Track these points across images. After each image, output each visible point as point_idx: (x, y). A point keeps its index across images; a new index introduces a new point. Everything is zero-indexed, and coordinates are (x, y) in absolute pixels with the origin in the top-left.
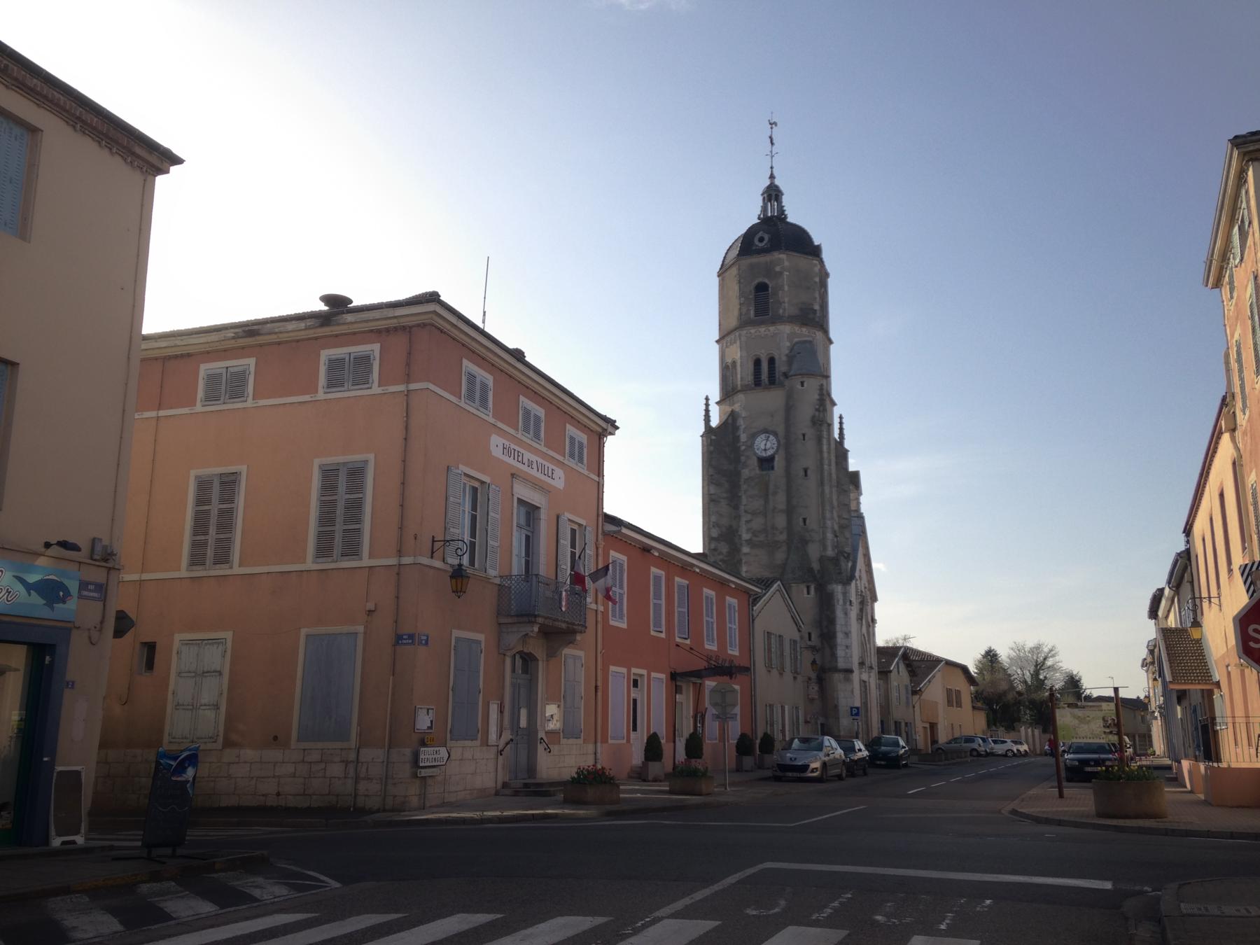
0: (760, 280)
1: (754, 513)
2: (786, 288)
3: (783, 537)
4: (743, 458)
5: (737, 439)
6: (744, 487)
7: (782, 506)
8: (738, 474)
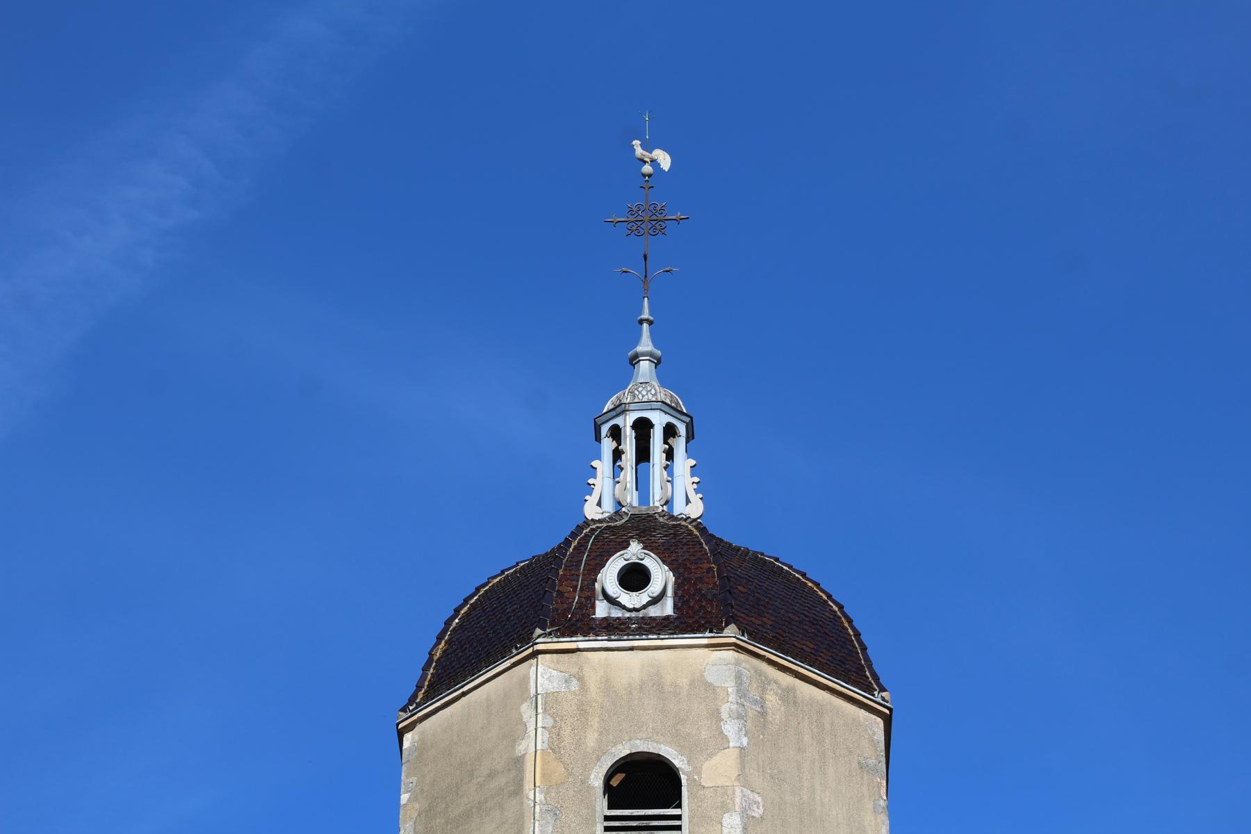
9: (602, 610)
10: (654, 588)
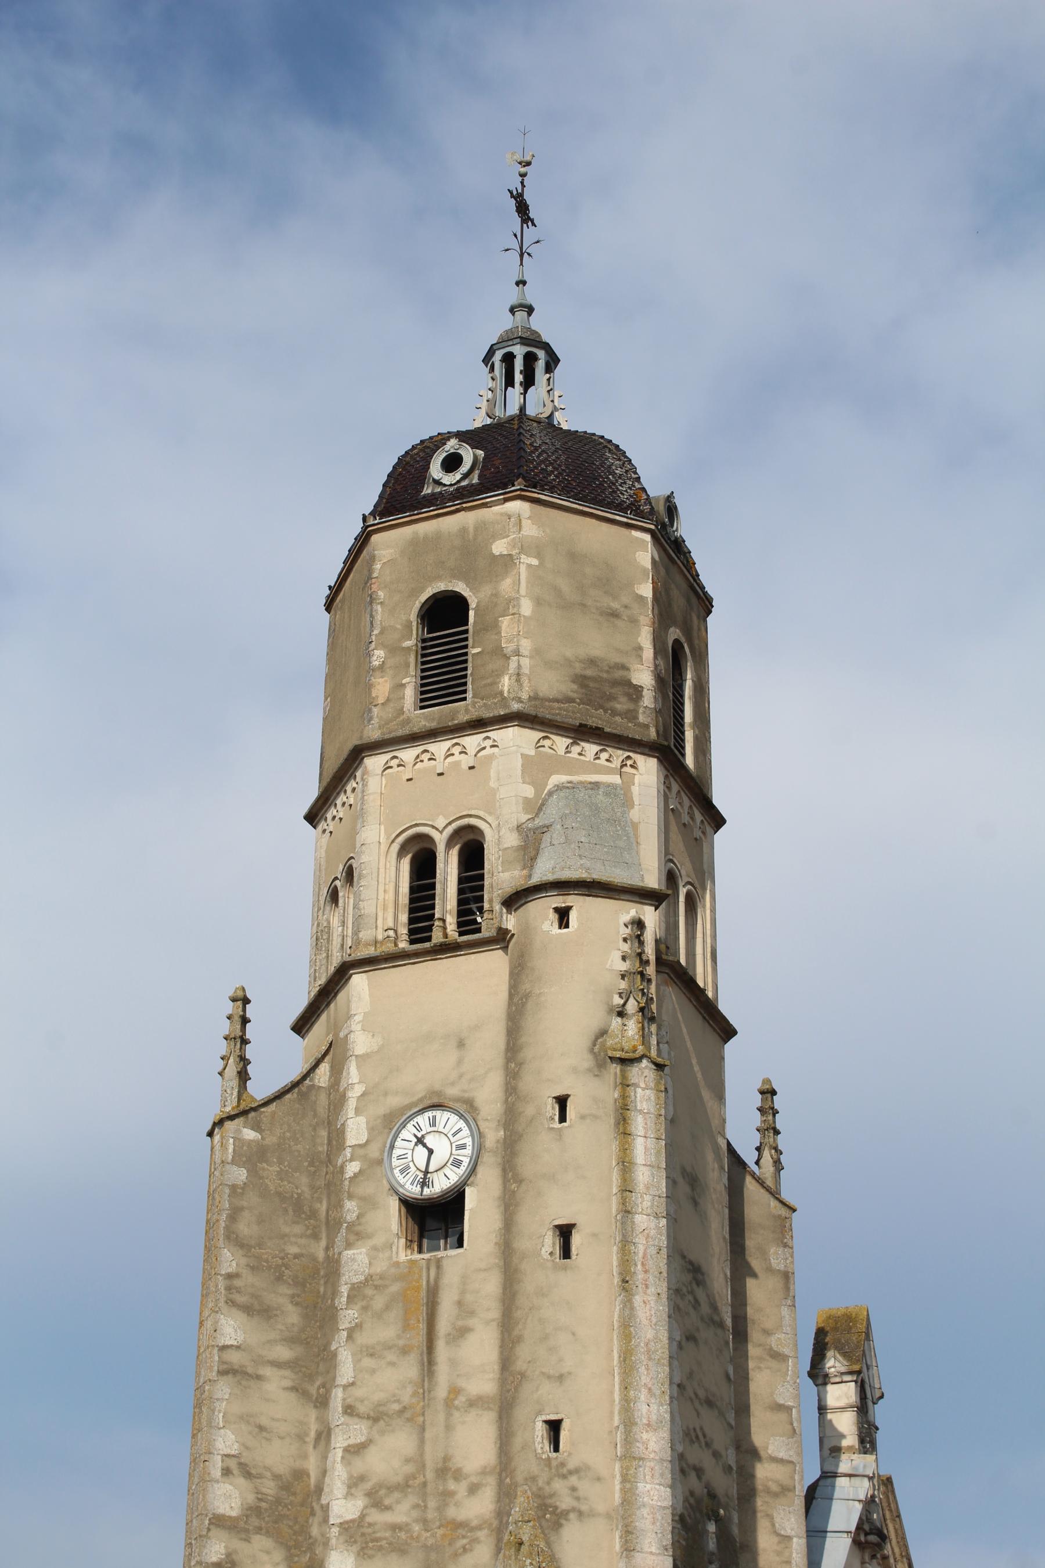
0: (441, 586)
1: (376, 1417)
2: (526, 608)
3: (479, 1507)
4: (351, 1208)
5: (337, 1137)
6: (348, 1316)
7: (484, 1384)
8: (332, 1268)
9: (427, 490)
10: (465, 468)
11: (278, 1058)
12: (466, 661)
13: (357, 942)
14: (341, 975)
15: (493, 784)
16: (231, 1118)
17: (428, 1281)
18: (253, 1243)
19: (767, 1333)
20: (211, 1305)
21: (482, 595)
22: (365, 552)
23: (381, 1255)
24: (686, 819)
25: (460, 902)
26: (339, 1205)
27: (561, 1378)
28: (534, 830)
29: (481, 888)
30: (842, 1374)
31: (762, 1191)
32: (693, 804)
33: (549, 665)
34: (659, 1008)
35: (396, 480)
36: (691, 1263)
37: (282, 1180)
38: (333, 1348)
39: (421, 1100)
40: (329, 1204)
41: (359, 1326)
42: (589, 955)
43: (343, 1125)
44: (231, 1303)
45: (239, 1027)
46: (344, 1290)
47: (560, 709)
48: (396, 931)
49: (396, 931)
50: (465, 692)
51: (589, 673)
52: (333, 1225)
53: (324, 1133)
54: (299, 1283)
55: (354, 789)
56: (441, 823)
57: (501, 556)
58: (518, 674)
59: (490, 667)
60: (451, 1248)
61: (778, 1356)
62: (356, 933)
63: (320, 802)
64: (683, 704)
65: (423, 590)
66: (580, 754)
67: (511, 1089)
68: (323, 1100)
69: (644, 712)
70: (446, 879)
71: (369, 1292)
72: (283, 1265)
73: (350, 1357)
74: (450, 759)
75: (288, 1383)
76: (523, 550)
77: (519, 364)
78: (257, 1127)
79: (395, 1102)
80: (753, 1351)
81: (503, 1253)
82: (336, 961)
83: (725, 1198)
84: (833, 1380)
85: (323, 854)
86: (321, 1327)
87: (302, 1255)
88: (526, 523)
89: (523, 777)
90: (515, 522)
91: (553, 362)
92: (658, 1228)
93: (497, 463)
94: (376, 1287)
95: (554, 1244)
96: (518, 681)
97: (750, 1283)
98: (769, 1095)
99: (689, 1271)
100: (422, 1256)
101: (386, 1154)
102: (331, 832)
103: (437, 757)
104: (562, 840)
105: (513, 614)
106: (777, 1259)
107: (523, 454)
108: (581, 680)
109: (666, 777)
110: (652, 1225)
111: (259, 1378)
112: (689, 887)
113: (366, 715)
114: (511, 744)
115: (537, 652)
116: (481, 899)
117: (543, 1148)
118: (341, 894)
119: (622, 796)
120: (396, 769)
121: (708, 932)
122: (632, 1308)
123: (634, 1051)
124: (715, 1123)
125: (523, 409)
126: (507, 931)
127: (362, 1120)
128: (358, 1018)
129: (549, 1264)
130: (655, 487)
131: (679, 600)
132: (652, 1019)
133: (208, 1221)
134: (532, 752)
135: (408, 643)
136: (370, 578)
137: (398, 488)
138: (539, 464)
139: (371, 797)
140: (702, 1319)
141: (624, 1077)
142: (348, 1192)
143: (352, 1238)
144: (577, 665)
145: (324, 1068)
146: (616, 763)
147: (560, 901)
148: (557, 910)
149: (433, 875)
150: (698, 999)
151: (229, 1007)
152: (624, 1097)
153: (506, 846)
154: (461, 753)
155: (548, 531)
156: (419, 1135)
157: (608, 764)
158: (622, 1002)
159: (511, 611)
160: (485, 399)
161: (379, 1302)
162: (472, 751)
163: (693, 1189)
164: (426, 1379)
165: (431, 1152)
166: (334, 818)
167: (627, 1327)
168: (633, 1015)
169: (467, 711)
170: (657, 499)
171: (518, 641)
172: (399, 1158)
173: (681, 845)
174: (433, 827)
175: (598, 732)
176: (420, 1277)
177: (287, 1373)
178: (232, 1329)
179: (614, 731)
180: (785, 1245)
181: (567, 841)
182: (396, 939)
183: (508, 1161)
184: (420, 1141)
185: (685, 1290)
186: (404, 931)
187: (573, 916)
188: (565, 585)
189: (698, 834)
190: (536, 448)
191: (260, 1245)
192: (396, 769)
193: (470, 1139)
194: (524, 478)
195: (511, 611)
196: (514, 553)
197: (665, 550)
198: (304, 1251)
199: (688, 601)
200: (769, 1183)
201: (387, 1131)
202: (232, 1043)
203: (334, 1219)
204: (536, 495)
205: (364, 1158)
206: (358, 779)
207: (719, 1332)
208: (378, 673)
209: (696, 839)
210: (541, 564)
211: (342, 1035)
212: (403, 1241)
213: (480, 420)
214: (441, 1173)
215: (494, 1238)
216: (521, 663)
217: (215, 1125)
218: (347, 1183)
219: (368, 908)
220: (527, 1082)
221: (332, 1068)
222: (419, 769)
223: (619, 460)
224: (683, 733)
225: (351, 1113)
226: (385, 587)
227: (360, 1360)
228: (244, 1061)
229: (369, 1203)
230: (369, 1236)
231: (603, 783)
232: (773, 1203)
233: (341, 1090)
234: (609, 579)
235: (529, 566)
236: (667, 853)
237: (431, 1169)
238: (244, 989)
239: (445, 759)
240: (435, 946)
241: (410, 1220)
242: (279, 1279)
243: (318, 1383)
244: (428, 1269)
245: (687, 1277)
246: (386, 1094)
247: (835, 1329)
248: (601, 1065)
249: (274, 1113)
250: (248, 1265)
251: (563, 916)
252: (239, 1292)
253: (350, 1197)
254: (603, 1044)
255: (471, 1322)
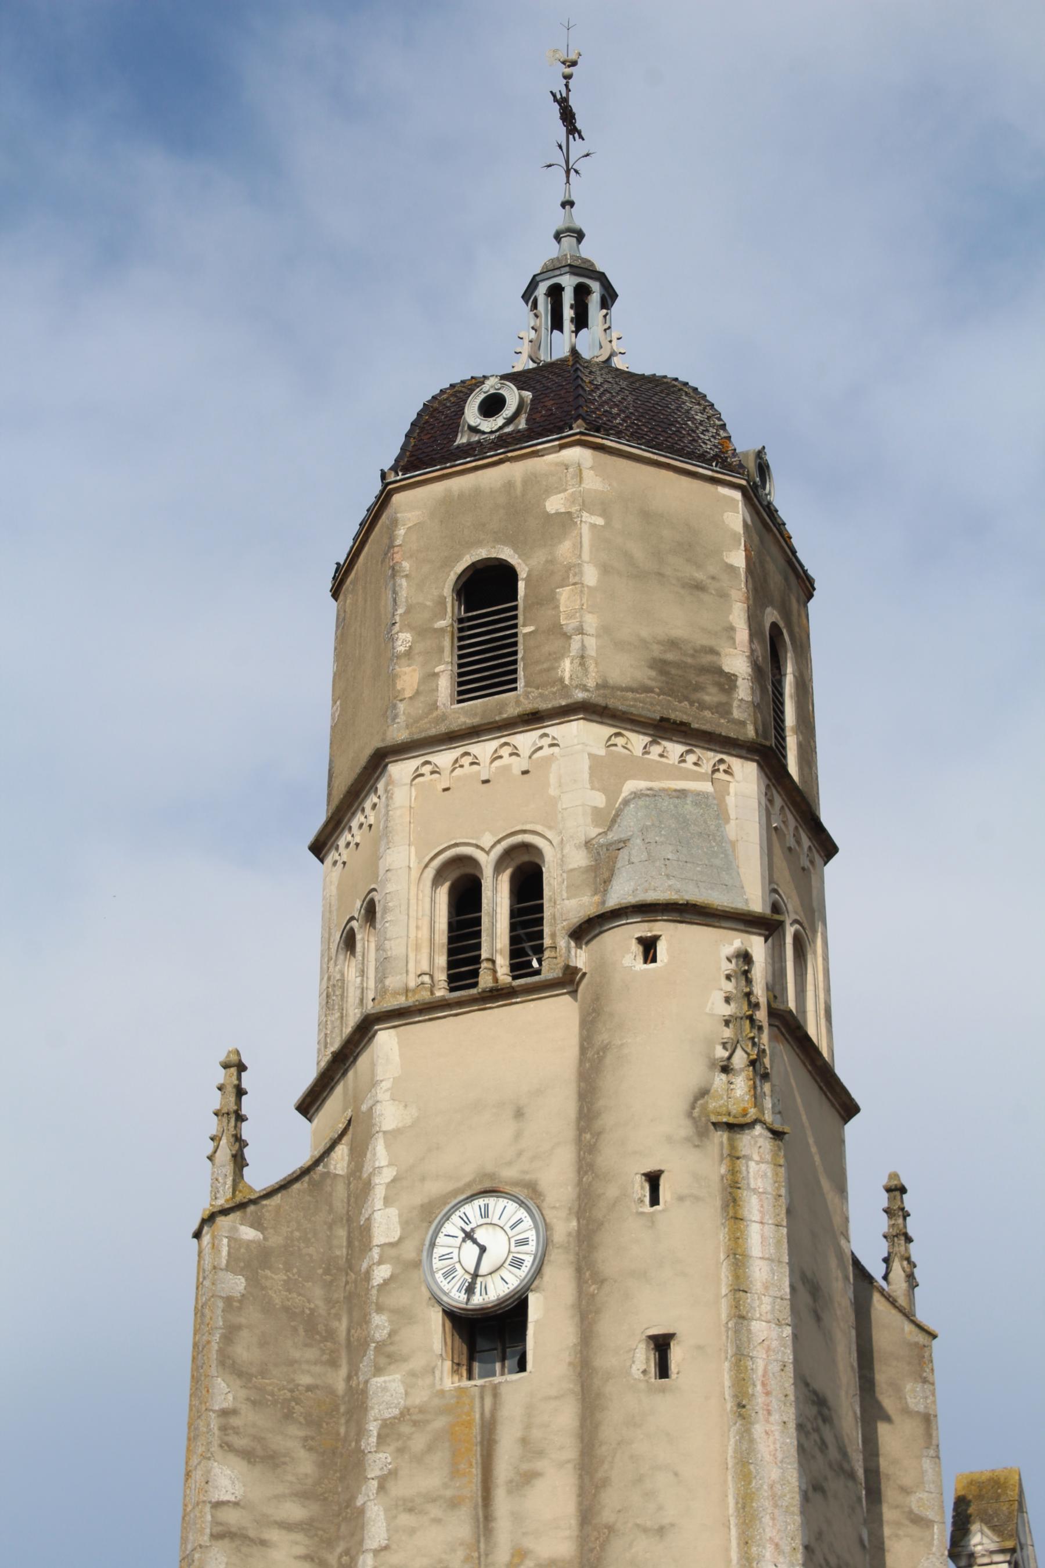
0: (482, 553)
2: (591, 576)
4: (380, 1324)
5: (360, 1236)
6: (379, 1462)
8: (357, 1401)
9: (462, 439)
11: (280, 1144)
12: (515, 644)
13: (382, 991)
14: (364, 1032)
15: (553, 791)
16: (225, 1212)
17: (482, 1414)
18: (254, 1370)
19: (905, 1491)
20: (200, 1450)
21: (533, 562)
22: (384, 517)
23: (420, 1382)
24: (791, 842)
25: (514, 940)
26: (365, 1320)
27: (661, 1531)
28: (608, 846)
29: (540, 921)
30: (992, 1552)
31: (894, 1311)
32: (801, 827)
33: (620, 646)
34: (772, 1061)
35: (422, 429)
36: (815, 1393)
37: (289, 1290)
38: (359, 1502)
39: (469, 1185)
40: (350, 1321)
41: (393, 1473)
42: (682, 995)
43: (368, 1219)
44: (227, 1447)
45: (233, 1099)
46: (373, 1428)
47: (635, 700)
48: (432, 977)
49: (432, 977)
50: (515, 681)
51: (670, 656)
52: (356, 1347)
53: (342, 1233)
54: (311, 1422)
55: (374, 806)
56: (487, 841)
57: (558, 514)
58: (582, 657)
59: (546, 649)
60: (510, 1372)
61: (918, 1520)
62: (380, 979)
63: (330, 826)
64: (782, 704)
65: (458, 559)
66: (661, 756)
67: (586, 1165)
68: (340, 1191)
69: (739, 706)
70: (494, 911)
71: (405, 1429)
72: (293, 1399)
73: (382, 1513)
74: (497, 763)
75: (301, 1550)
76: (584, 507)
77: (568, 298)
78: (257, 1224)
79: (435, 1188)
80: (888, 1514)
81: (580, 1375)
82: (353, 1017)
83: (852, 1317)
84: (980, 1561)
85: (334, 890)
86: (342, 1479)
87: (317, 1387)
88: (588, 474)
89: (591, 782)
90: (575, 474)
91: (609, 297)
92: (781, 1338)
93: (549, 404)
94: (415, 1423)
95: (648, 1360)
96: (582, 664)
97: (882, 1428)
98: (898, 1193)
99: (813, 1403)
100: (473, 1383)
101: (425, 1254)
102: (344, 863)
103: (481, 760)
104: (644, 856)
105: (574, 584)
106: (914, 1396)
107: (581, 392)
108: (660, 666)
109: (768, 787)
110: (774, 1335)
111: (263, 1543)
112: (797, 926)
113: (389, 712)
114: (576, 741)
115: (605, 631)
116: (540, 935)
117: (633, 1237)
118: (358, 937)
119: (714, 807)
120: (428, 777)
121: (821, 985)
122: (752, 1441)
123: (745, 1115)
124: (837, 1220)
125: (574, 351)
126: (575, 970)
127: (393, 1212)
128: (385, 1085)
129: (642, 1386)
130: (744, 442)
131: (776, 579)
132: (765, 1076)
133: (195, 1345)
134: (602, 752)
135: (442, 623)
136: (391, 546)
137: (425, 438)
138: (602, 405)
139: (398, 812)
140: (830, 1465)
141: (732, 1147)
142: (377, 1304)
143: (382, 1361)
144: (655, 647)
145: (342, 1151)
146: (707, 768)
147: (645, 930)
148: (640, 940)
149: (478, 907)
150: (813, 1062)
151: (220, 1076)
152: (733, 1172)
153: (571, 867)
154: (511, 755)
155: (615, 484)
156: (468, 1229)
157: (695, 768)
158: (726, 1054)
159: (572, 580)
160: (526, 341)
161: (419, 1442)
162: (525, 750)
163: (815, 1301)
164: (482, 1540)
165: (483, 1249)
166: (348, 844)
167: (745, 1465)
168: (742, 1070)
169: (518, 703)
170: (746, 454)
171: (581, 616)
172: (442, 1258)
173: (787, 874)
174: (478, 847)
175: (683, 728)
176: (472, 1408)
177: (299, 1537)
178: (228, 1480)
179: (704, 727)
180: (925, 1381)
181: (650, 858)
182: (433, 986)
183: (585, 1257)
184: (469, 1236)
185: (809, 1426)
186: (442, 976)
187: (661, 948)
188: (638, 552)
189: (806, 863)
190: (597, 387)
191: (263, 1373)
192: (428, 777)
193: (534, 1232)
194: (584, 419)
195: (572, 580)
196: (573, 510)
197: (758, 513)
198: (319, 1382)
199: (786, 579)
200: (902, 1301)
201: (425, 1224)
202: (225, 1120)
203: (358, 1340)
204: (599, 441)
205: (397, 1261)
206: (379, 792)
207: (850, 1484)
208: (403, 661)
209: (803, 869)
210: (608, 524)
211: (364, 1108)
212: (448, 1364)
213: (523, 364)
214: (496, 1276)
215: (566, 1357)
216: (586, 643)
217: (204, 1222)
218: (374, 1292)
219: (396, 948)
220: (607, 1157)
221: (352, 1150)
222: (459, 778)
223: (699, 404)
224: (784, 739)
225: (379, 1204)
226: (411, 556)
227: (395, 1517)
228: (240, 1142)
229: (404, 1316)
230: (405, 1359)
231: (692, 792)
232: (908, 1327)
233: (365, 1176)
234: (691, 545)
235: (593, 526)
236: (771, 881)
237: (483, 1271)
238: (238, 1053)
239: (492, 761)
240: (484, 991)
241: (457, 1337)
242: (288, 1416)
243: (339, 1550)
244: (482, 1398)
245: (814, 1410)
246: (423, 1179)
247: (980, 1497)
248: (702, 1134)
249: (278, 1207)
250: (248, 1399)
251: (649, 947)
252: (237, 1433)
253: (380, 1309)
254: (704, 1107)
255: (539, 1465)
